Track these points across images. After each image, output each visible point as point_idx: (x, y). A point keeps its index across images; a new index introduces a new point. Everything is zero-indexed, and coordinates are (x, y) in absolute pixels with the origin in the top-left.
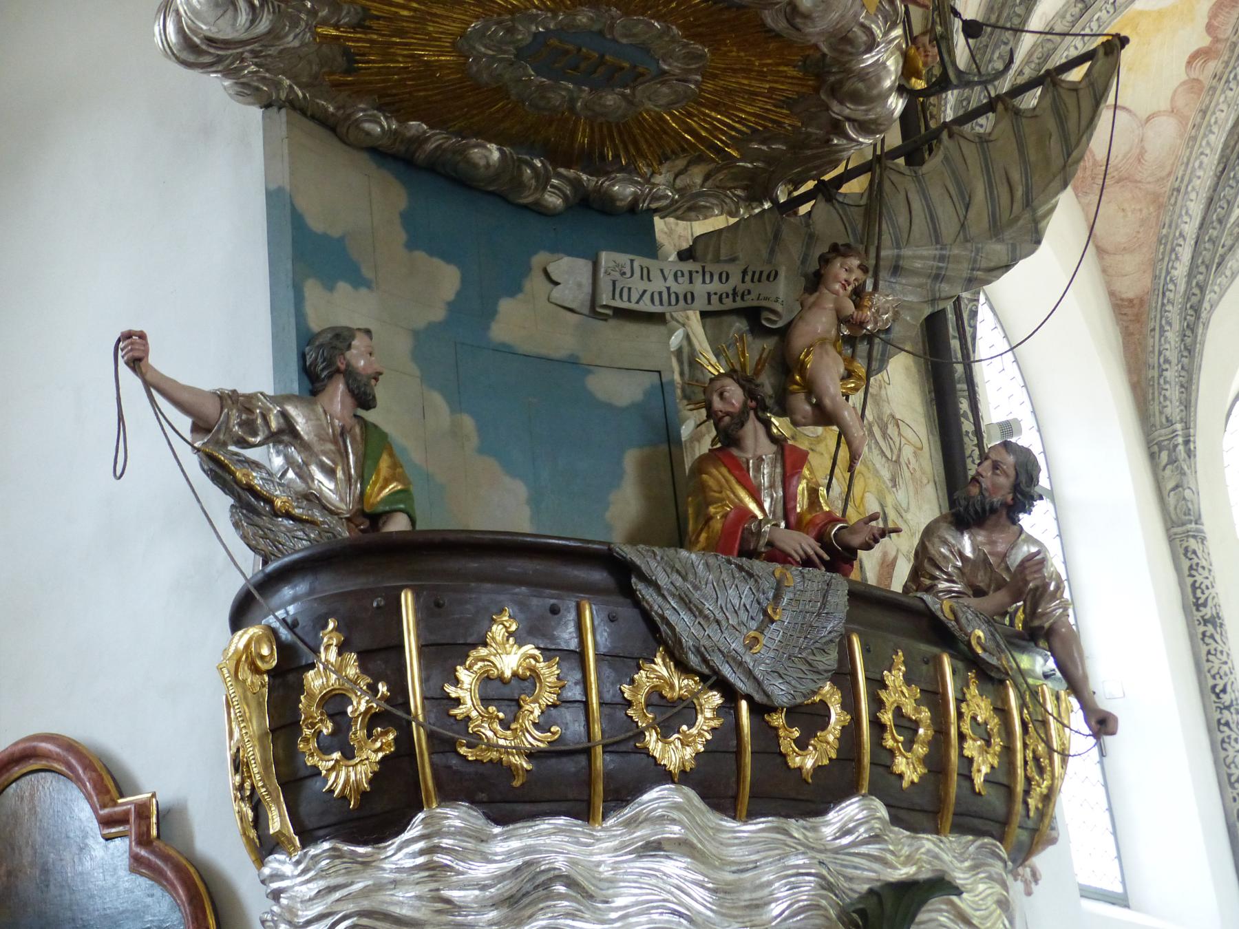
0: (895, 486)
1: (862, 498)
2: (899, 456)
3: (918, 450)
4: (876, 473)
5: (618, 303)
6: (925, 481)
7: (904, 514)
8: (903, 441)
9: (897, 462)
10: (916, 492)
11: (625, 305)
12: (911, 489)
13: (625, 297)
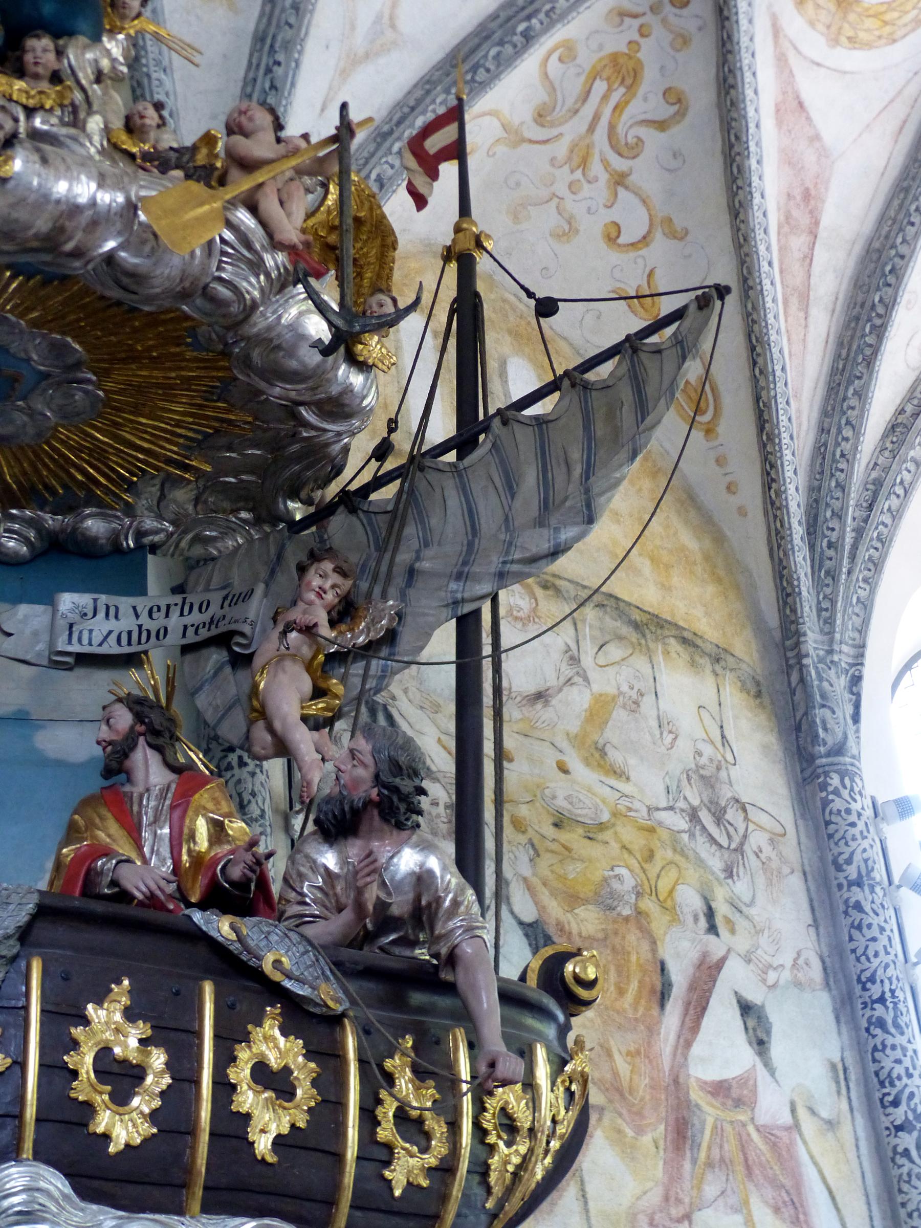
0: (731, 876)
1: (671, 892)
2: (742, 844)
3: (775, 839)
4: (700, 863)
5: (75, 648)
6: (786, 870)
7: (744, 909)
8: (751, 827)
9: (740, 849)
10: (770, 883)
11: (86, 649)
12: (761, 880)
13: (85, 641)
